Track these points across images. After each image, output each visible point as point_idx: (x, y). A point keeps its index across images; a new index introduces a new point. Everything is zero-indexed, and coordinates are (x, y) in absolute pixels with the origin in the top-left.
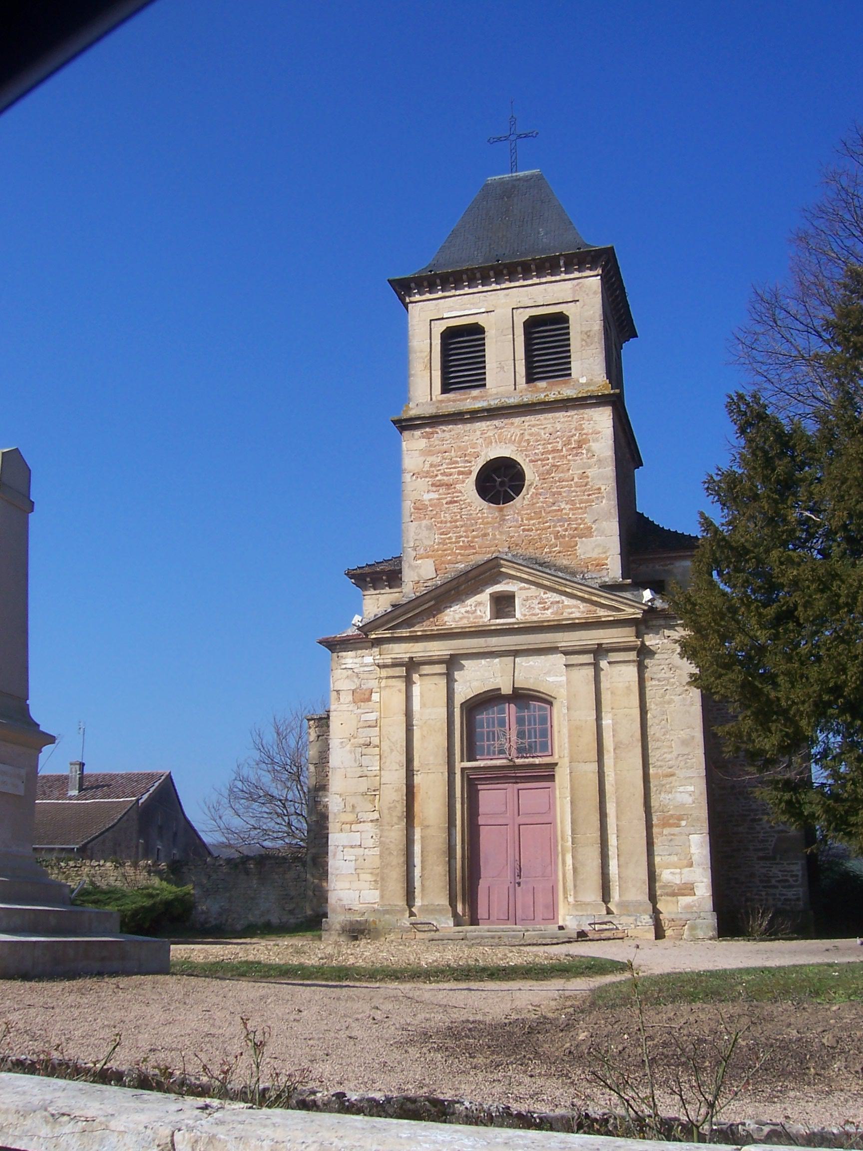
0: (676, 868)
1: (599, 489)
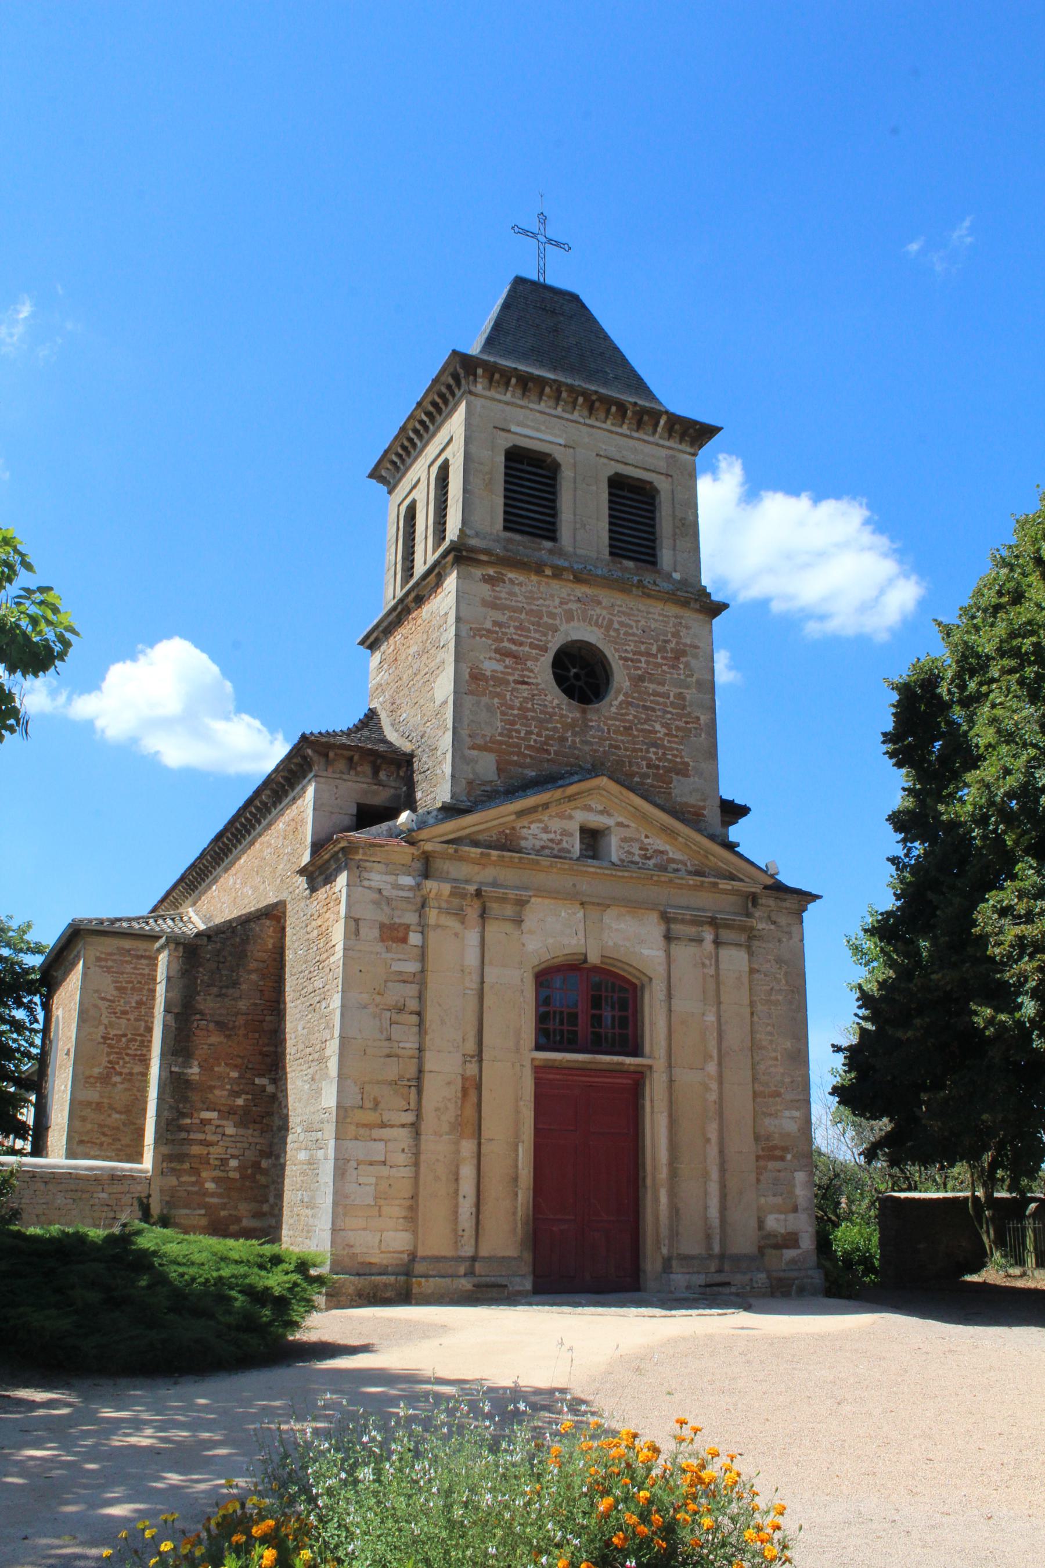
1: (698, 718)
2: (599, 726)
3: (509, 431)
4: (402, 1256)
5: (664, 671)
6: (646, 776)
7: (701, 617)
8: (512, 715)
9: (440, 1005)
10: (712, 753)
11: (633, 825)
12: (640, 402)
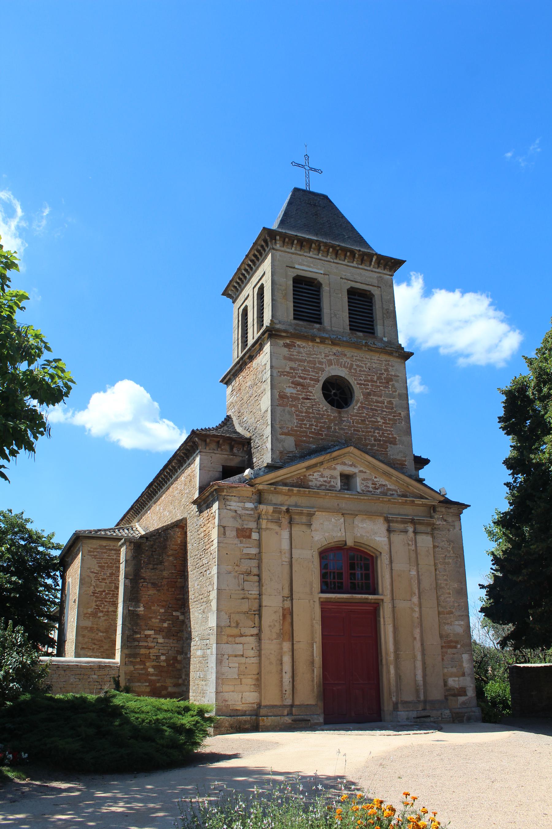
0: (456, 677)
1: (400, 414)
2: (348, 420)
3: (294, 268)
4: (253, 705)
5: (381, 390)
6: (373, 445)
7: (399, 360)
8: (302, 416)
9: (269, 571)
10: (408, 432)
11: (368, 471)
12: (362, 250)
